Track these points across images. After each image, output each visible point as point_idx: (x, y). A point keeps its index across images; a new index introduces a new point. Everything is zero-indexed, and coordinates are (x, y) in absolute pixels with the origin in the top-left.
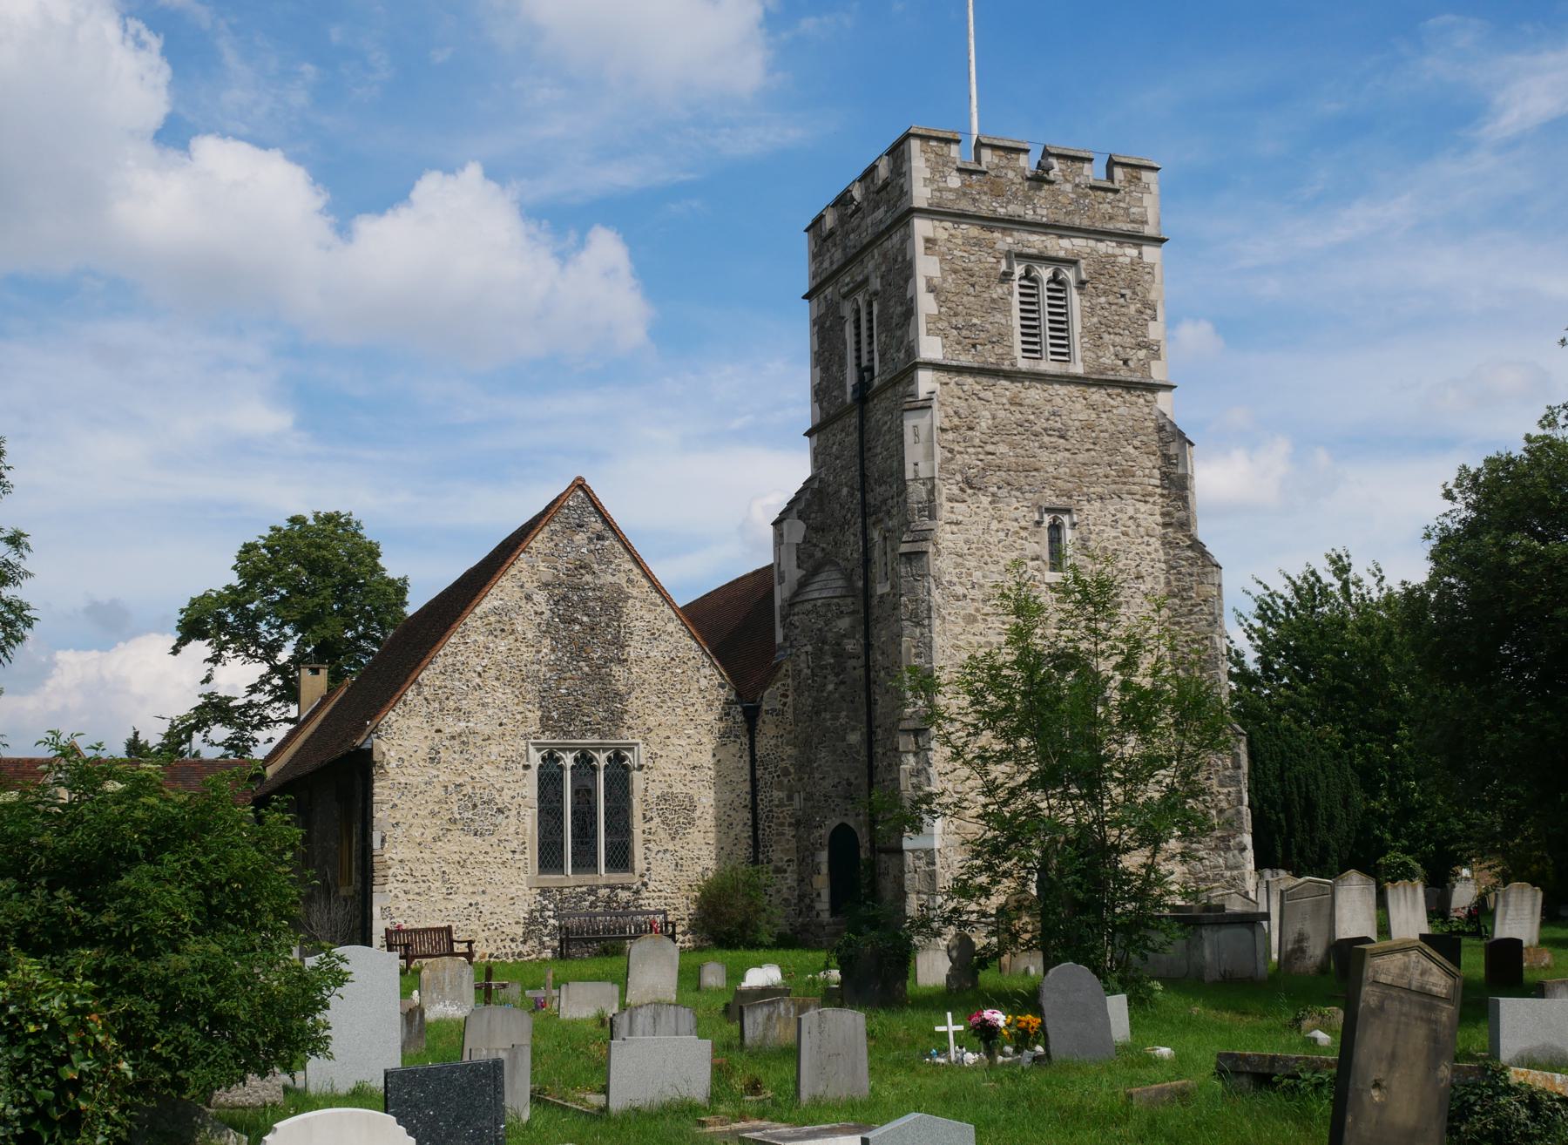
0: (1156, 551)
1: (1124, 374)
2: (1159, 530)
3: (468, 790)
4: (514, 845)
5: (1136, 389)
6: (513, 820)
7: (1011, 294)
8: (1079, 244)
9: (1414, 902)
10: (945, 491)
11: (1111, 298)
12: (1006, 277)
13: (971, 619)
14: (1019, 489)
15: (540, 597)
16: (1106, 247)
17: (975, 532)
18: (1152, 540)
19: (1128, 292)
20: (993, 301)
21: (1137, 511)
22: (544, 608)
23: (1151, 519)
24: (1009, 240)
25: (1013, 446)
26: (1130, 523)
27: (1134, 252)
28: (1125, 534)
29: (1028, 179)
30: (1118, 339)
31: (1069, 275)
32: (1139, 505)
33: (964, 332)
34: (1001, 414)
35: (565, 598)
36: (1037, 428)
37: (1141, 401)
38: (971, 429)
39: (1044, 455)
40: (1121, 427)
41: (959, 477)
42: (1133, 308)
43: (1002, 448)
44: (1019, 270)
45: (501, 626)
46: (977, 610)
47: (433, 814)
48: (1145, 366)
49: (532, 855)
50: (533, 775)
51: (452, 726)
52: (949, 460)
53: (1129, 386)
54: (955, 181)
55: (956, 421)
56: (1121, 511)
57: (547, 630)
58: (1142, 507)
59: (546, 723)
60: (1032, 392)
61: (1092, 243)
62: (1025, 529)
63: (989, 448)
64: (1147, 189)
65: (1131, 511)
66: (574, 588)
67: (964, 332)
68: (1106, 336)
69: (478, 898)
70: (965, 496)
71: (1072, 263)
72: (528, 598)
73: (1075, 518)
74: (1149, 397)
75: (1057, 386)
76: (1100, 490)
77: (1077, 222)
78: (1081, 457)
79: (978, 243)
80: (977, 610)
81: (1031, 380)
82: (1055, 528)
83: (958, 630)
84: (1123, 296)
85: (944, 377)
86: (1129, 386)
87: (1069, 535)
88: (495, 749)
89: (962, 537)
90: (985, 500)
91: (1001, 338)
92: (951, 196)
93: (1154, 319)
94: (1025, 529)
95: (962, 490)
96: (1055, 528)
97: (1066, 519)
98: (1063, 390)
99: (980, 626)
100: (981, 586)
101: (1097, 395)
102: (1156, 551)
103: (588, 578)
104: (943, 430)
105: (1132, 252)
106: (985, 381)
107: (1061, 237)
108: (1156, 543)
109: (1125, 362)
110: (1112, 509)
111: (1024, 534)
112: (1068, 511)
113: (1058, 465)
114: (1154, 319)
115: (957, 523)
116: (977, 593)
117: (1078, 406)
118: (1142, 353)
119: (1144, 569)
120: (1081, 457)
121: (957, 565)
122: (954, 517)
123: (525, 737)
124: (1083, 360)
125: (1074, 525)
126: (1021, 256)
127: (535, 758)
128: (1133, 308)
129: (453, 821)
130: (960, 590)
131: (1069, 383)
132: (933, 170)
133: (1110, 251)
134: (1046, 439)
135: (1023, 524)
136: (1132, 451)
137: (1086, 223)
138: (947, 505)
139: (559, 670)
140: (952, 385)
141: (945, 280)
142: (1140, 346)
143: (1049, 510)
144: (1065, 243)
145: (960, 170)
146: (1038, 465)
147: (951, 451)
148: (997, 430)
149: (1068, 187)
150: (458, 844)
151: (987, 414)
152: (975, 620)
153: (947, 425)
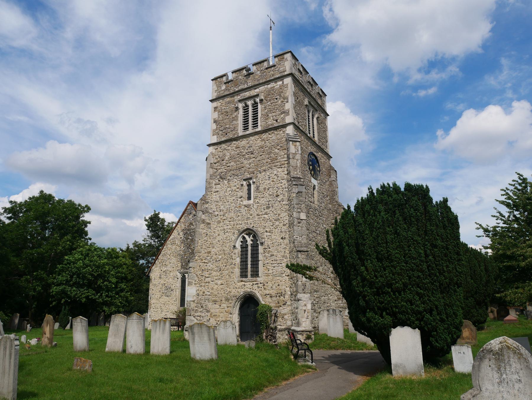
0: (285, 184)
1: (276, 125)
2: (286, 176)
3: (166, 285)
4: (174, 299)
5: (279, 129)
6: (174, 293)
7: (238, 114)
8: (262, 88)
9: (164, 330)
10: (214, 182)
11: (272, 102)
12: (237, 109)
13: (219, 222)
14: (236, 176)
15: (181, 234)
16: (272, 85)
17: (222, 194)
18: (282, 181)
19: (278, 97)
20: (233, 118)
21: (278, 172)
22: (182, 236)
23: (283, 173)
24: (239, 97)
25: (235, 162)
26: (275, 177)
27: (281, 83)
28: (273, 181)
29: (246, 76)
30: (274, 114)
31: (258, 100)
32: (278, 169)
33: (224, 131)
34: (233, 152)
35: (187, 233)
36: (244, 154)
37: (281, 132)
38: (223, 160)
39: (245, 162)
40: (273, 144)
41: (218, 177)
42: (280, 101)
43: (232, 163)
44: (241, 106)
45: (173, 244)
46: (221, 219)
47: (160, 291)
48: (283, 119)
49: (178, 302)
50: (180, 280)
51: (164, 269)
52: (216, 172)
53: (276, 128)
54: (224, 87)
55: (219, 159)
56: (272, 173)
57: (183, 242)
58: (280, 170)
59: (182, 266)
60: (243, 142)
61: (266, 86)
62: (238, 188)
63: (228, 165)
64: (287, 60)
65: (275, 172)
66: (188, 230)
67: (224, 131)
68: (270, 115)
69: (167, 313)
70: (220, 182)
71: (257, 96)
72: (179, 234)
73: (254, 180)
74: (284, 129)
75: (251, 138)
76: (264, 168)
77: (261, 82)
78: (257, 159)
79: (229, 102)
80: (221, 219)
81: (242, 138)
82: (249, 186)
83: (215, 226)
84: (277, 99)
85: (216, 147)
86: (276, 128)
87: (253, 187)
88: (172, 274)
89: (218, 196)
90: (226, 182)
91: (235, 129)
92: (222, 92)
93: (287, 102)
94: (238, 188)
95: (219, 181)
96: (249, 186)
97: (251, 182)
98: (252, 138)
99: (222, 224)
100: (223, 210)
101: (264, 136)
102: (285, 184)
103: (192, 227)
104: (215, 163)
105: (280, 83)
106: (228, 144)
107: (255, 89)
108: (285, 182)
109: (277, 121)
110: (268, 174)
111: (237, 190)
112: (251, 179)
113: (250, 164)
114: (287, 102)
115: (217, 191)
116: (222, 213)
117: (258, 141)
118: (282, 116)
119: (280, 192)
120: (257, 159)
121: (216, 205)
122: (216, 190)
123: (178, 270)
124: (261, 126)
125: (254, 182)
126: (240, 101)
127: (180, 276)
128: (280, 101)
129: (163, 293)
130: (216, 213)
131: (255, 135)
132: (218, 87)
133: (272, 86)
134: (247, 156)
135: (238, 186)
136: (276, 150)
137: (264, 81)
138: (214, 186)
139: (184, 252)
140: (219, 149)
141: (219, 117)
142: (282, 113)
143: (244, 180)
144: (257, 90)
145: (225, 83)
146: (243, 165)
147: (216, 169)
148: (232, 158)
149: (259, 72)
150: (165, 299)
151: (228, 154)
152: (220, 222)
153: (216, 161)
